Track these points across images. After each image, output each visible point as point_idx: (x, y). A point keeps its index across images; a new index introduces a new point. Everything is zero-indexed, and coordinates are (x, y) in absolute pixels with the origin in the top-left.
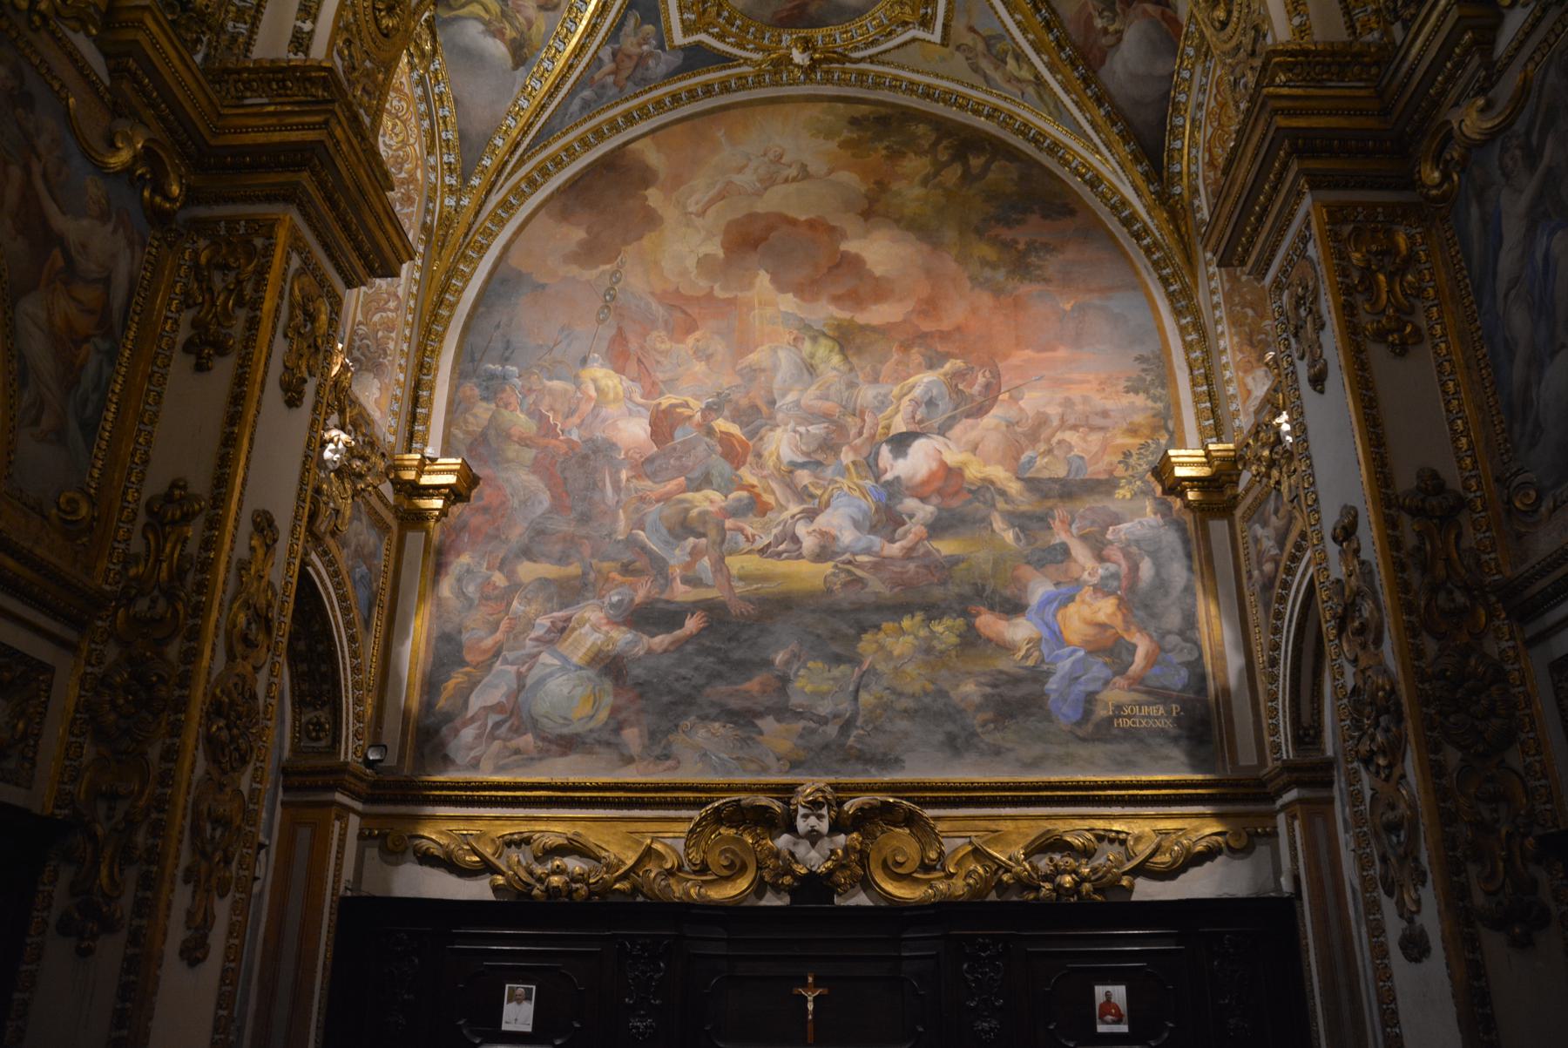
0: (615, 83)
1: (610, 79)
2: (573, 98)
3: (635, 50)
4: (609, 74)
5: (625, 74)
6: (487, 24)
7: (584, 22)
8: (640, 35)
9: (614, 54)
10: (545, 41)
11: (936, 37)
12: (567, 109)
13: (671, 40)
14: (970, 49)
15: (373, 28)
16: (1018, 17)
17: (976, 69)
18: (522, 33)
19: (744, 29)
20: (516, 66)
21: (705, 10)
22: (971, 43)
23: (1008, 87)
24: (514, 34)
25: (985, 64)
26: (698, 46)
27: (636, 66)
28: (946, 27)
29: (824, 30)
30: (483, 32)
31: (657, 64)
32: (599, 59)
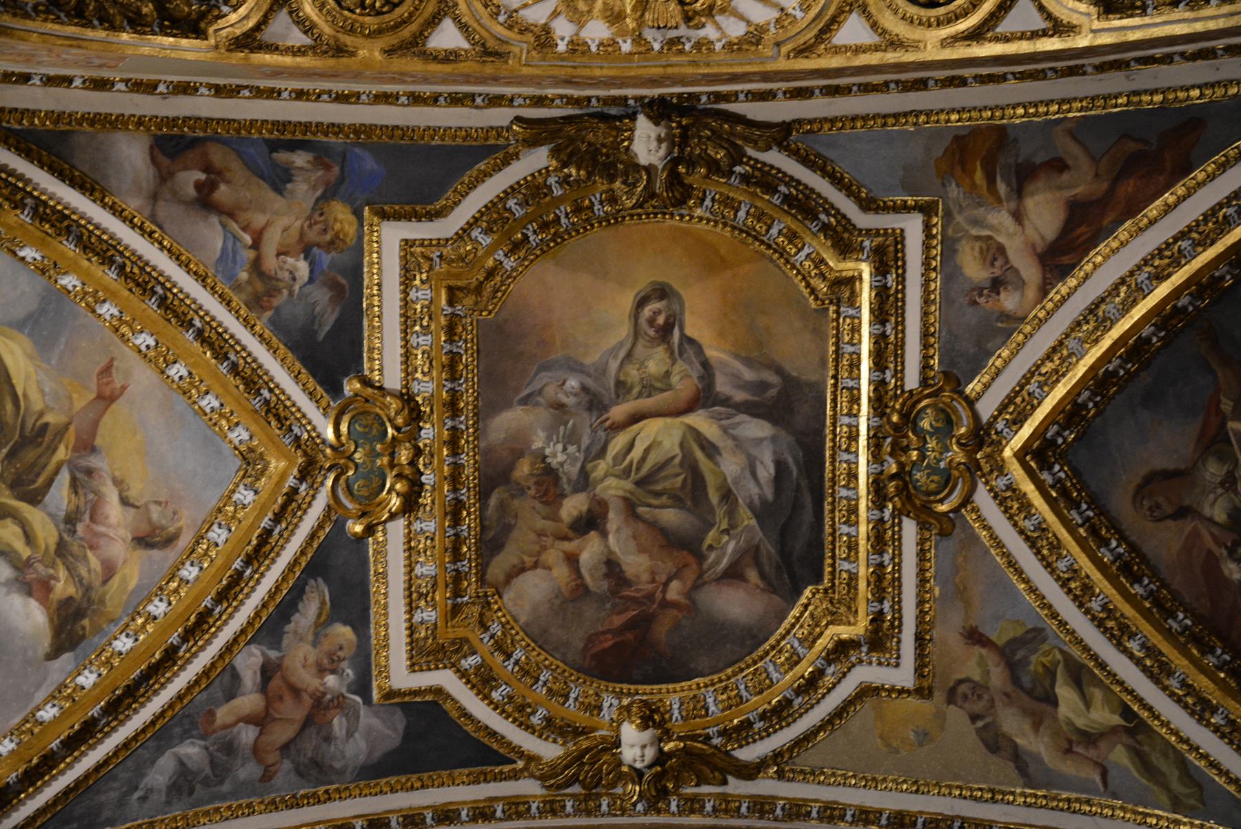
0: (256, 750)
1: (248, 734)
2: (160, 751)
3: (307, 679)
4: (249, 720)
5: (281, 734)
6: (21, 566)
8: (326, 645)
9: (268, 671)
11: (904, 676)
12: (140, 773)
13: (385, 671)
14: (979, 689)
17: (995, 742)
18: (88, 589)
20: (56, 652)
22: (977, 677)
23: (1068, 767)
24: (72, 591)
25: (1012, 723)
27: (308, 722)
30: (7, 583)
31: (350, 734)
32: (235, 677)
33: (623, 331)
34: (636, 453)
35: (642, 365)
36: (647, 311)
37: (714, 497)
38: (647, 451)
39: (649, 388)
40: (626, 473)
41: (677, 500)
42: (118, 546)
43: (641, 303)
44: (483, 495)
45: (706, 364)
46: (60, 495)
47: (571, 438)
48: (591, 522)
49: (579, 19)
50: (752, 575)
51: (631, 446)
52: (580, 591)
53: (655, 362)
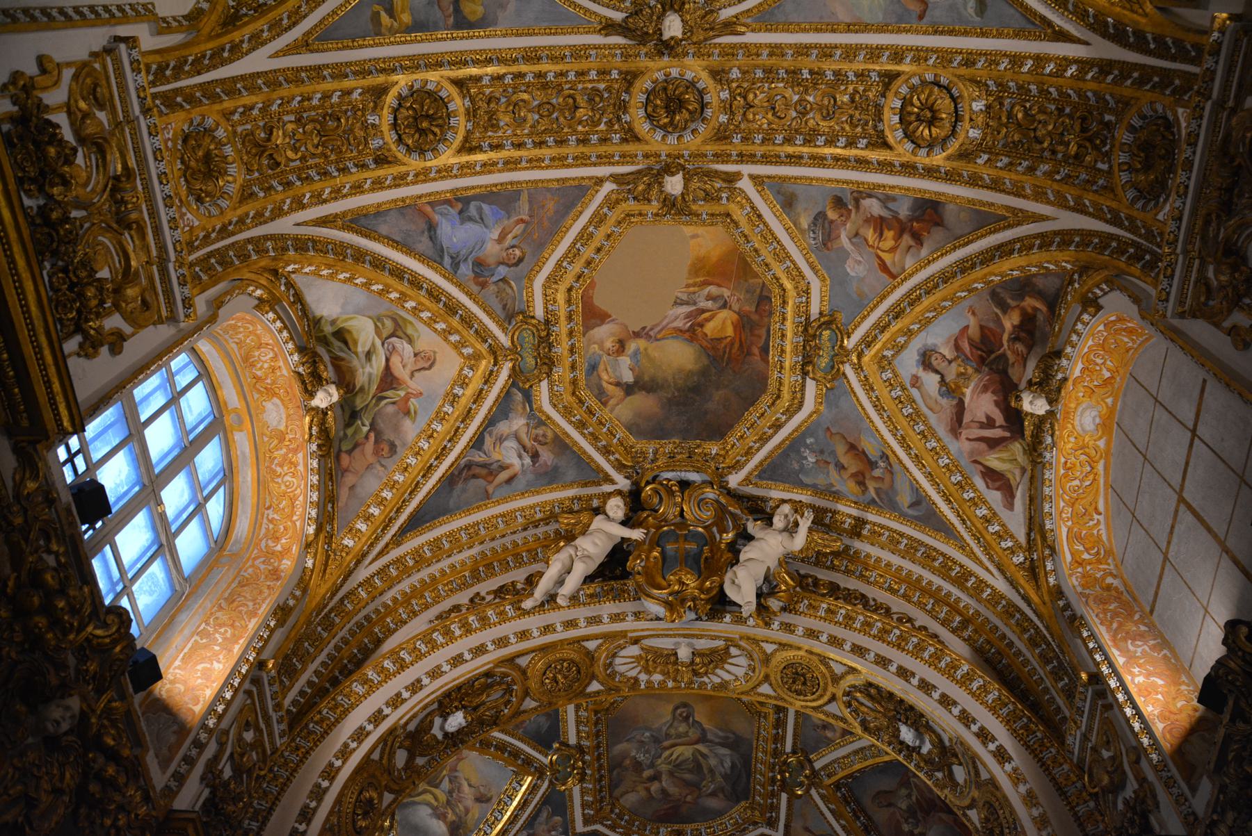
6: (435, 809)
7: (509, 813)
10: (476, 825)
15: (350, 827)
16: (843, 822)
18: (460, 818)
19: (631, 823)
21: (601, 808)
26: (595, 833)
28: (787, 826)
29: (694, 826)
33: (669, 717)
34: (674, 757)
35: (676, 729)
36: (679, 711)
37: (706, 771)
39: (679, 736)
40: (670, 763)
41: (690, 771)
42: (469, 802)
43: (676, 708)
44: (610, 771)
45: (703, 730)
46: (446, 784)
47: (647, 752)
48: (656, 777)
49: (648, 672)
50: (721, 795)
52: (651, 797)
53: (682, 728)
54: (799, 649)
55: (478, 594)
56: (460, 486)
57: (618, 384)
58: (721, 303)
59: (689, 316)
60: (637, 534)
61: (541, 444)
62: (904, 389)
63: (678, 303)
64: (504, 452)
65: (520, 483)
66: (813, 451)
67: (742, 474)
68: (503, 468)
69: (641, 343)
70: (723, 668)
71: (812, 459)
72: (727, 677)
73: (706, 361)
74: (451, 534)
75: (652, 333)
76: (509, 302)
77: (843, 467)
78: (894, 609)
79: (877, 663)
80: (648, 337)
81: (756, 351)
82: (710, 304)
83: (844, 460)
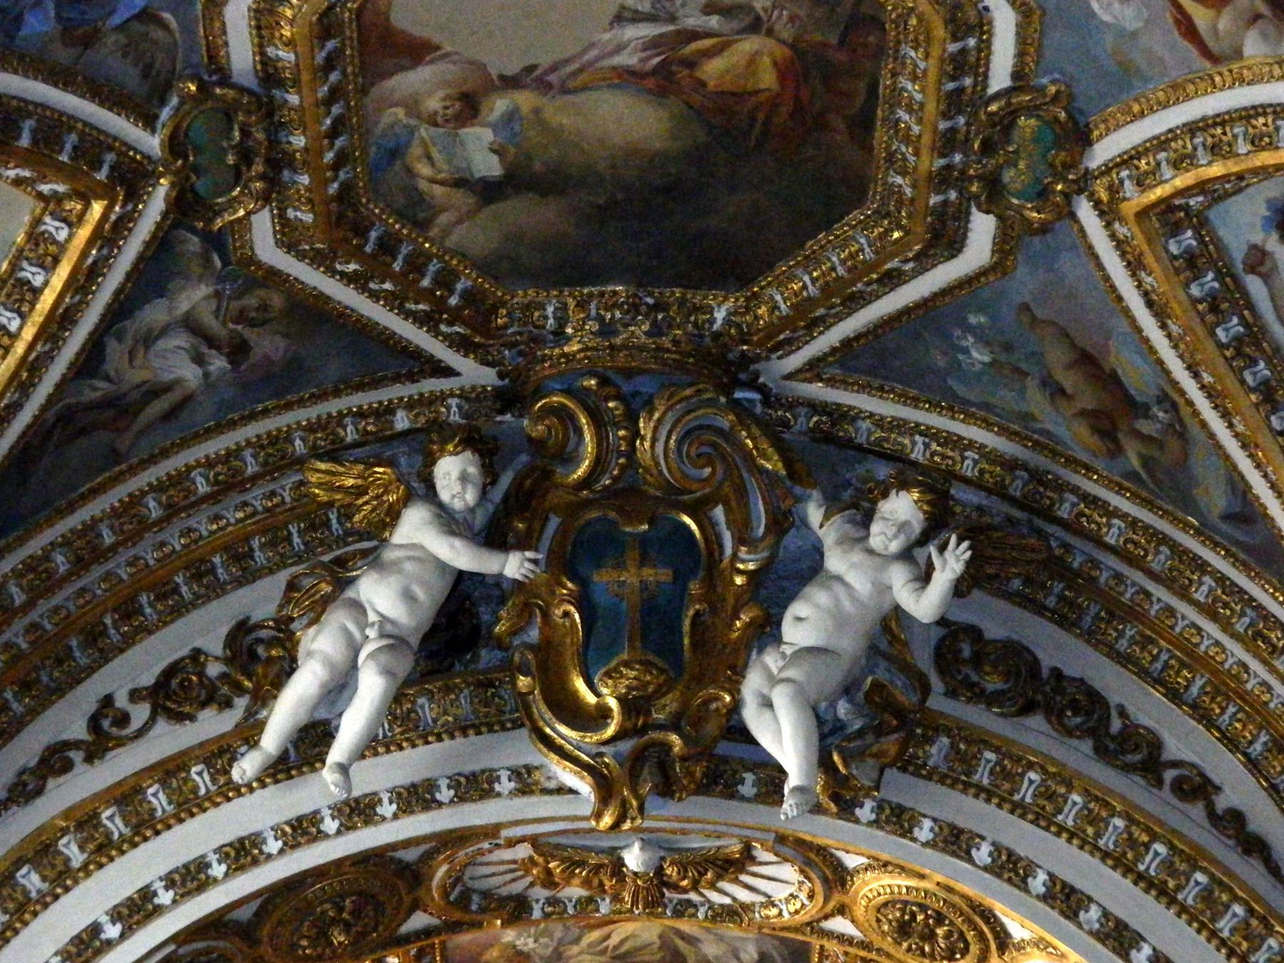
38: (622, 942)
51: (608, 937)
54: (922, 877)
55: (108, 701)
56: (46, 461)
57: (461, 183)
58: (747, 20)
59: (654, 44)
60: (514, 566)
61: (252, 324)
62: (1226, 274)
63: (623, 17)
64: (157, 363)
65: (203, 414)
66: (984, 340)
67: (796, 360)
68: (155, 391)
69: (525, 100)
70: (736, 881)
71: (980, 356)
72: (744, 896)
73: (702, 137)
74: (31, 565)
75: (553, 78)
76: (160, 57)
77: (1062, 391)
78: (1174, 748)
79: (1101, 937)
80: (543, 86)
81: (838, 123)
82: (714, 21)
83: (1068, 380)
